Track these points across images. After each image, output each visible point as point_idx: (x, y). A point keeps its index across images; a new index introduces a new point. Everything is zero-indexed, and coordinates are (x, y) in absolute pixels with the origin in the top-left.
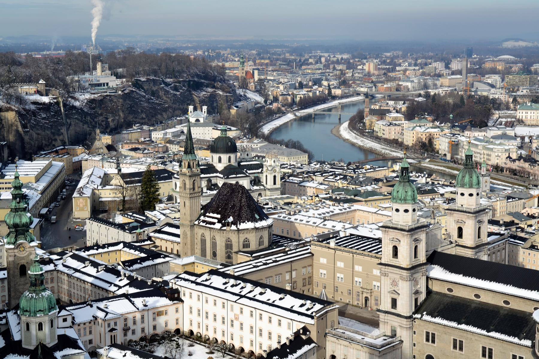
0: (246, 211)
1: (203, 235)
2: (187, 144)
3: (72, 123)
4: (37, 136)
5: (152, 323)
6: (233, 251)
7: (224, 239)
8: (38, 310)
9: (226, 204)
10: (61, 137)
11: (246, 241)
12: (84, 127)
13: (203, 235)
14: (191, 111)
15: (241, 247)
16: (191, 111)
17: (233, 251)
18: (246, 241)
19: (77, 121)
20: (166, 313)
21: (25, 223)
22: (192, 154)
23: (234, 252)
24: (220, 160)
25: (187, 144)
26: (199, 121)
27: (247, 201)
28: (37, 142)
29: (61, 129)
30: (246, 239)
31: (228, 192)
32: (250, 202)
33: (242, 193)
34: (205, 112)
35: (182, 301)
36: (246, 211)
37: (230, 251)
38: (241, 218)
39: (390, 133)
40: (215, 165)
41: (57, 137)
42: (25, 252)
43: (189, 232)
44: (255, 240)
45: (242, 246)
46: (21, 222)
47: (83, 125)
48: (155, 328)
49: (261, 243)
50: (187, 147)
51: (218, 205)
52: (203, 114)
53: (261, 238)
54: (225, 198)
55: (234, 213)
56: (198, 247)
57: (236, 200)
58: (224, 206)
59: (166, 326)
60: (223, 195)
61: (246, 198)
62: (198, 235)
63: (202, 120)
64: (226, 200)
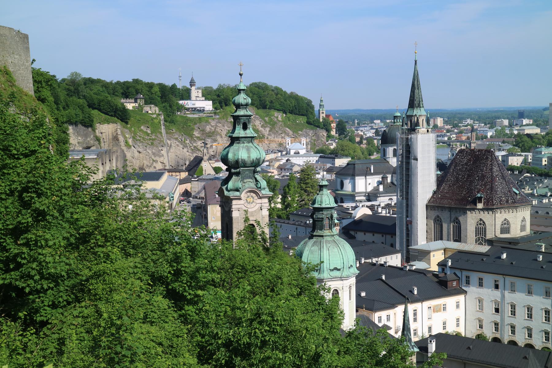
3: (172, 145)
5: (426, 324)
8: (332, 268)
9: (469, 176)
11: (505, 224)
12: (184, 150)
14: (288, 143)
18: (505, 224)
20: (444, 309)
22: (421, 107)
26: (299, 153)
27: (500, 170)
29: (162, 150)
31: (470, 160)
41: (157, 158)
42: (254, 204)
46: (249, 157)
47: (183, 149)
48: (430, 329)
49: (523, 228)
51: (457, 178)
53: (524, 220)
54: (466, 168)
55: (485, 185)
58: (467, 178)
59: (444, 328)
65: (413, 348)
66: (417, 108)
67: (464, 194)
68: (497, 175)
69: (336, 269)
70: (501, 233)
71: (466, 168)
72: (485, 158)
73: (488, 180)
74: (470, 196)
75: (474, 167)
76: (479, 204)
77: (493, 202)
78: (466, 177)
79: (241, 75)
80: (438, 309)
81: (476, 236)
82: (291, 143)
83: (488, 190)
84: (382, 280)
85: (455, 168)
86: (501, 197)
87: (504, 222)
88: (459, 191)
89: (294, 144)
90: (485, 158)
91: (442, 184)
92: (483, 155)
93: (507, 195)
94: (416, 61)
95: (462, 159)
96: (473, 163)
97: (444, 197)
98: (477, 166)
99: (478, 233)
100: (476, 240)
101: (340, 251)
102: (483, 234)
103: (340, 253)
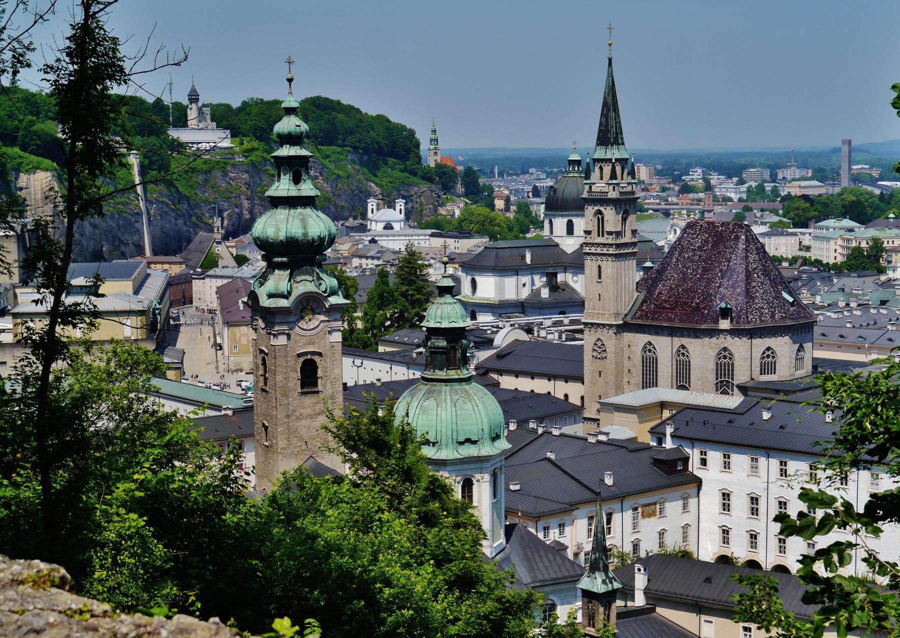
0: (762, 283)
1: (648, 348)
2: (607, 121)
4: (91, 229)
5: (630, 538)
6: (736, 383)
7: (713, 353)
8: (461, 439)
9: (705, 270)
10: (136, 238)
11: (768, 356)
12: (178, 222)
13: (648, 348)
14: (373, 209)
15: (756, 370)
16: (373, 209)
17: (736, 383)
18: (768, 356)
19: (166, 209)
21: (316, 238)
22: (619, 144)
23: (739, 387)
24: (570, 230)
25: (607, 121)
26: (392, 228)
27: (760, 260)
28: (91, 242)
30: (768, 349)
31: (706, 242)
32: (766, 262)
33: (747, 240)
34: (401, 210)
35: (698, 482)
36: (762, 283)
37: (728, 382)
38: (753, 298)
39: (777, 249)
40: (557, 240)
43: (613, 342)
44: (788, 354)
45: (759, 369)
47: (176, 219)
50: (607, 126)
52: (396, 214)
54: (700, 256)
56: (632, 381)
57: (733, 257)
58: (702, 275)
60: (694, 250)
61: (758, 253)
62: (633, 348)
63: (397, 226)
64: (704, 261)
65: (612, 583)
66: (612, 145)
67: (696, 303)
68: (756, 268)
69: (468, 441)
70: (761, 374)
71: (700, 256)
72: (733, 237)
73: (738, 277)
74: (707, 306)
75: (715, 255)
76: (723, 321)
77: (748, 318)
78: (699, 271)
79: (290, 80)
80: (650, 512)
81: (717, 379)
82: (378, 209)
83: (739, 295)
84: (549, 460)
85: (680, 255)
86: (762, 308)
87: (767, 353)
88: (688, 298)
89: (382, 211)
90: (733, 237)
91: (657, 286)
92: (730, 232)
93: (773, 304)
94: (610, 60)
95: (693, 239)
96: (712, 246)
97: (660, 308)
98: (719, 253)
99: (721, 374)
100: (717, 387)
101: (476, 408)
102: (729, 375)
103: (477, 412)
